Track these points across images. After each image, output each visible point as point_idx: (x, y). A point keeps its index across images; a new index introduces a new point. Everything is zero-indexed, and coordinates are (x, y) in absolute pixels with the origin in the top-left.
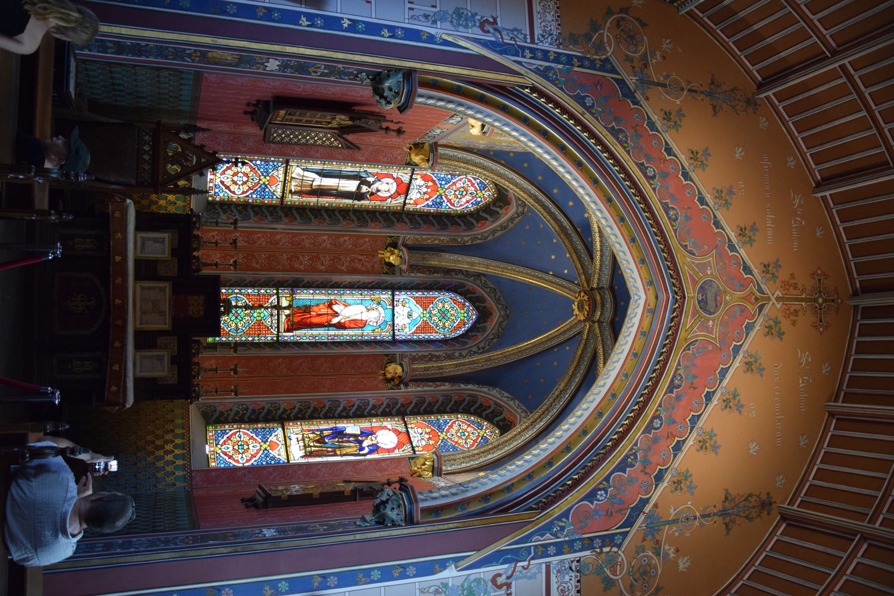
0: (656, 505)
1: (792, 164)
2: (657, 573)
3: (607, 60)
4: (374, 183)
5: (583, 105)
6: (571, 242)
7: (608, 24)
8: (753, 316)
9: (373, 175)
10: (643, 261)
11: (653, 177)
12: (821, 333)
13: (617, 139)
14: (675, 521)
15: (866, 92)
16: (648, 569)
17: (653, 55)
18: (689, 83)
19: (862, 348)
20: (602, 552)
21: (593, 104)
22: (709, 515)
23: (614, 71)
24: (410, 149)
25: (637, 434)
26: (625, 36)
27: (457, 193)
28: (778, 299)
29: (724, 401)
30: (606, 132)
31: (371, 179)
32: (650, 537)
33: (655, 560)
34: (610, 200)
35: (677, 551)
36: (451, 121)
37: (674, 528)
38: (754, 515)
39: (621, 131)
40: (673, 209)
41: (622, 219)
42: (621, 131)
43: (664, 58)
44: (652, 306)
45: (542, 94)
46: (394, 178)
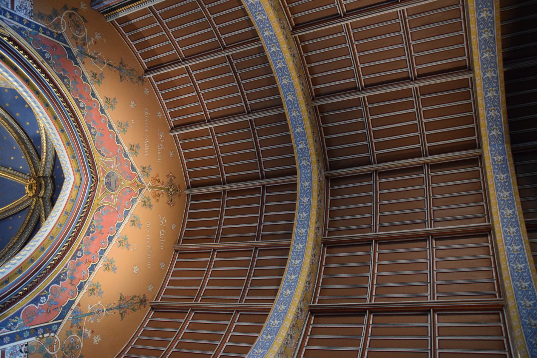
0: (79, 305)
1: (160, 116)
2: (80, 348)
3: (61, 35)
5: (44, 57)
6: (26, 148)
7: (64, 14)
8: (136, 195)
10: (74, 157)
11: (83, 108)
12: (171, 207)
13: (63, 82)
14: (91, 314)
15: (197, 83)
16: (74, 345)
17: (89, 40)
18: (108, 60)
19: (191, 216)
20: (43, 337)
21: (50, 58)
22: (111, 309)
23: (65, 42)
25: (67, 260)
26: (74, 24)
28: (149, 187)
29: (119, 242)
30: (56, 76)
32: (75, 324)
33: (79, 339)
34: (55, 118)
35: (93, 332)
37: (91, 318)
38: (136, 308)
39: (66, 78)
40: (94, 128)
41: (62, 131)
42: (66, 78)
43: (96, 43)
44: (78, 184)
45: (16, 43)
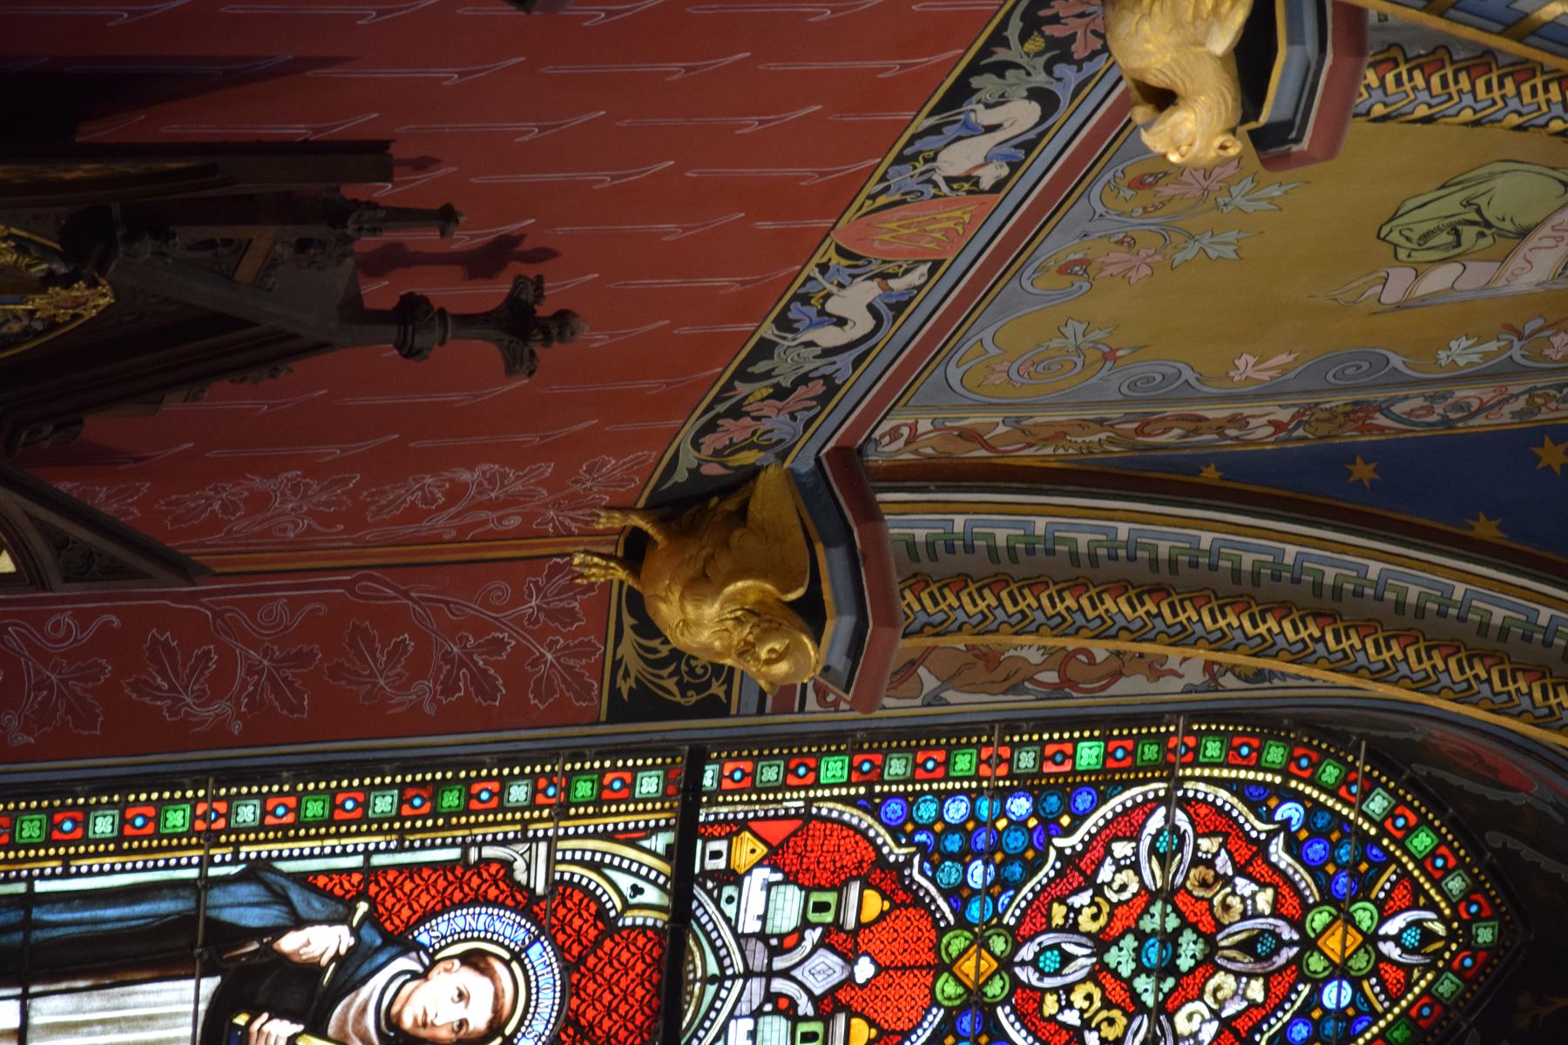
4: (352, 969)
9: (332, 895)
24: (635, 551)
27: (1121, 958)
31: (321, 942)
36: (958, 158)
46: (523, 902)
